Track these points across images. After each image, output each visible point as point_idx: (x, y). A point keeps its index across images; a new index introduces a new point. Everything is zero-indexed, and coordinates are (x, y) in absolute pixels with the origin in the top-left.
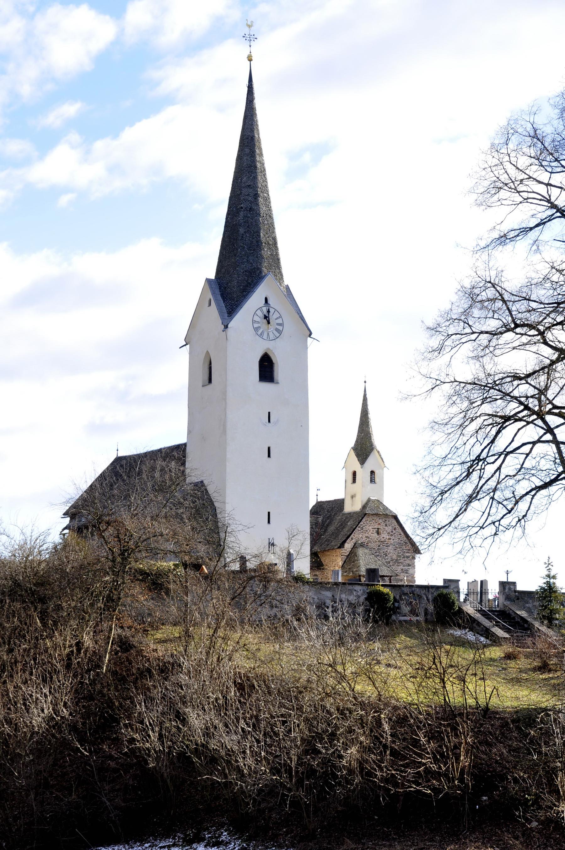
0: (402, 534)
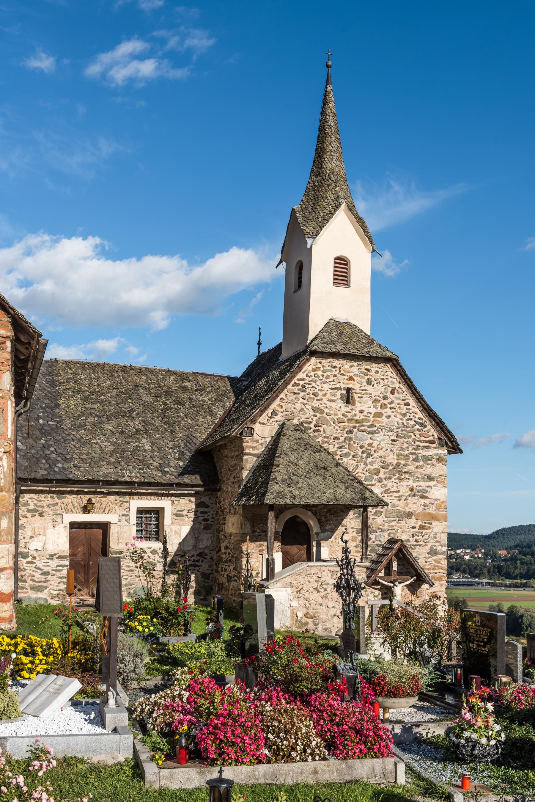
0: (412, 402)
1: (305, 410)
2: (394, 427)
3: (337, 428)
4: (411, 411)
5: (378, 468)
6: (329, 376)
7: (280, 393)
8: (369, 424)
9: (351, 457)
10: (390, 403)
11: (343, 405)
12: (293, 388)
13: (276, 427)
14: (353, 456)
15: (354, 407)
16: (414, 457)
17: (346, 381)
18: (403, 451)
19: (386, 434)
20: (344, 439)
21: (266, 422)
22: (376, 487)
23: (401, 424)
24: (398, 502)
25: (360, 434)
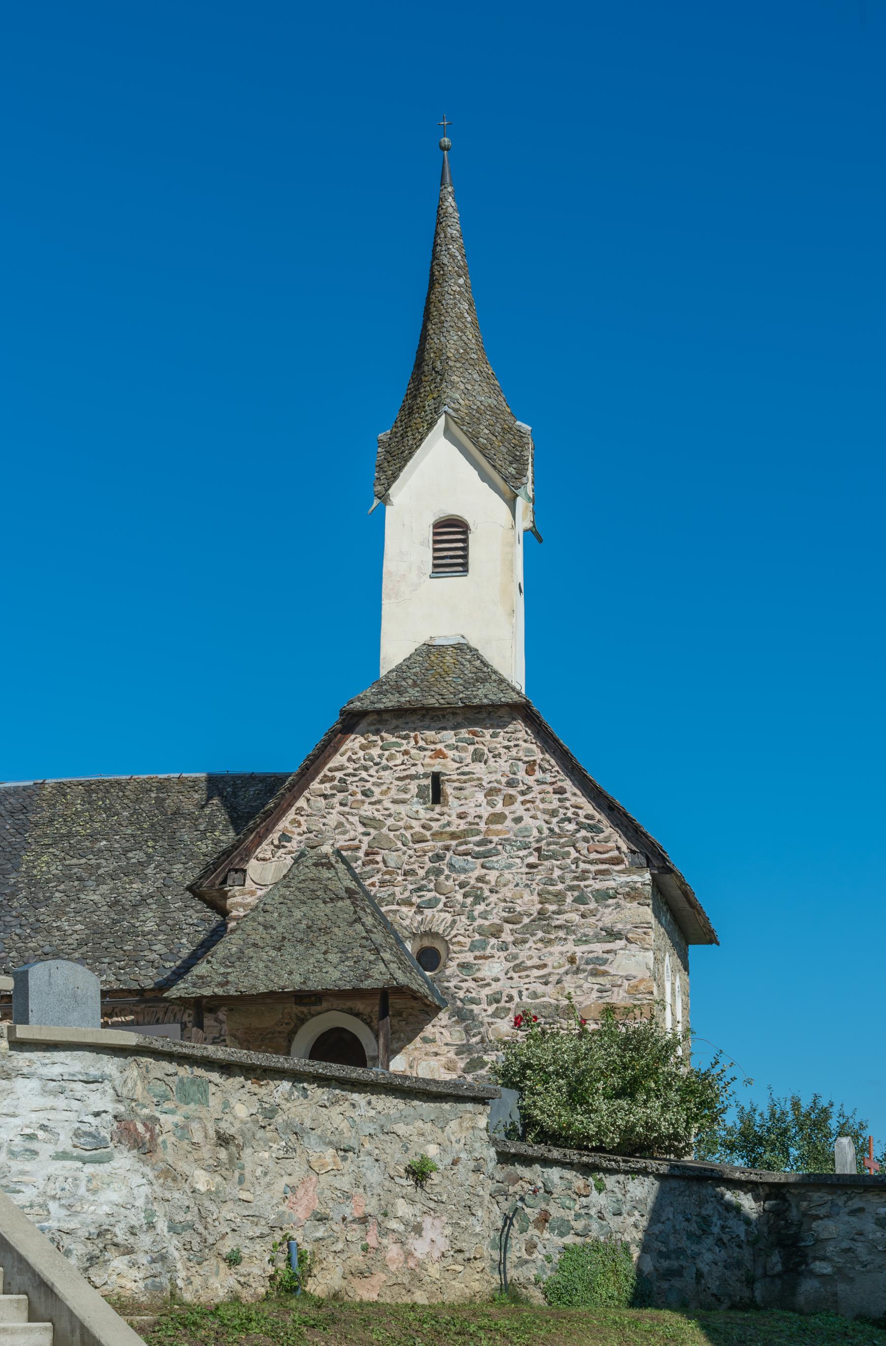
1: (346, 824)
2: (531, 839)
3: (411, 852)
4: (568, 804)
5: (499, 922)
6: (392, 754)
7: (296, 798)
8: (477, 838)
9: (441, 906)
10: (523, 793)
11: (420, 808)
12: (322, 786)
13: (289, 861)
14: (445, 905)
15: (445, 809)
16: (576, 894)
17: (427, 761)
18: (554, 885)
19: (513, 853)
20: (427, 873)
21: (268, 855)
22: (496, 960)
23: (546, 832)
24: (543, 987)
25: (459, 861)
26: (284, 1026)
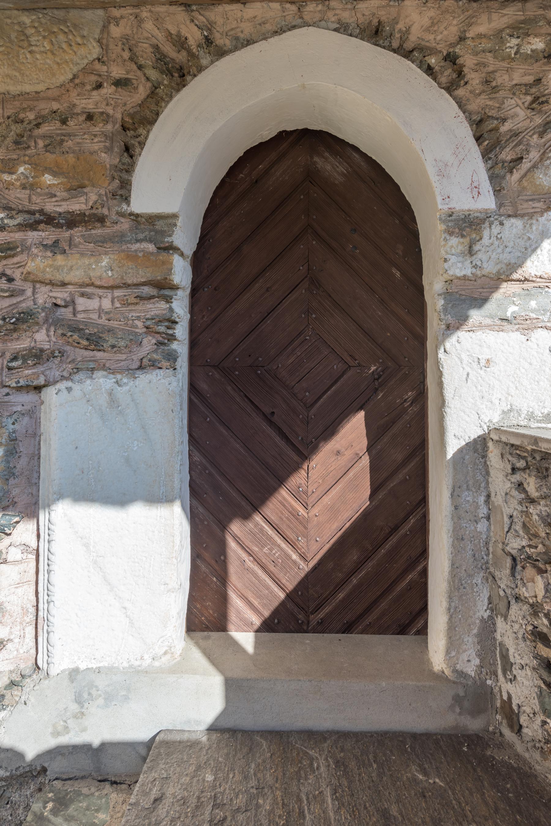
26: (108, 90)
